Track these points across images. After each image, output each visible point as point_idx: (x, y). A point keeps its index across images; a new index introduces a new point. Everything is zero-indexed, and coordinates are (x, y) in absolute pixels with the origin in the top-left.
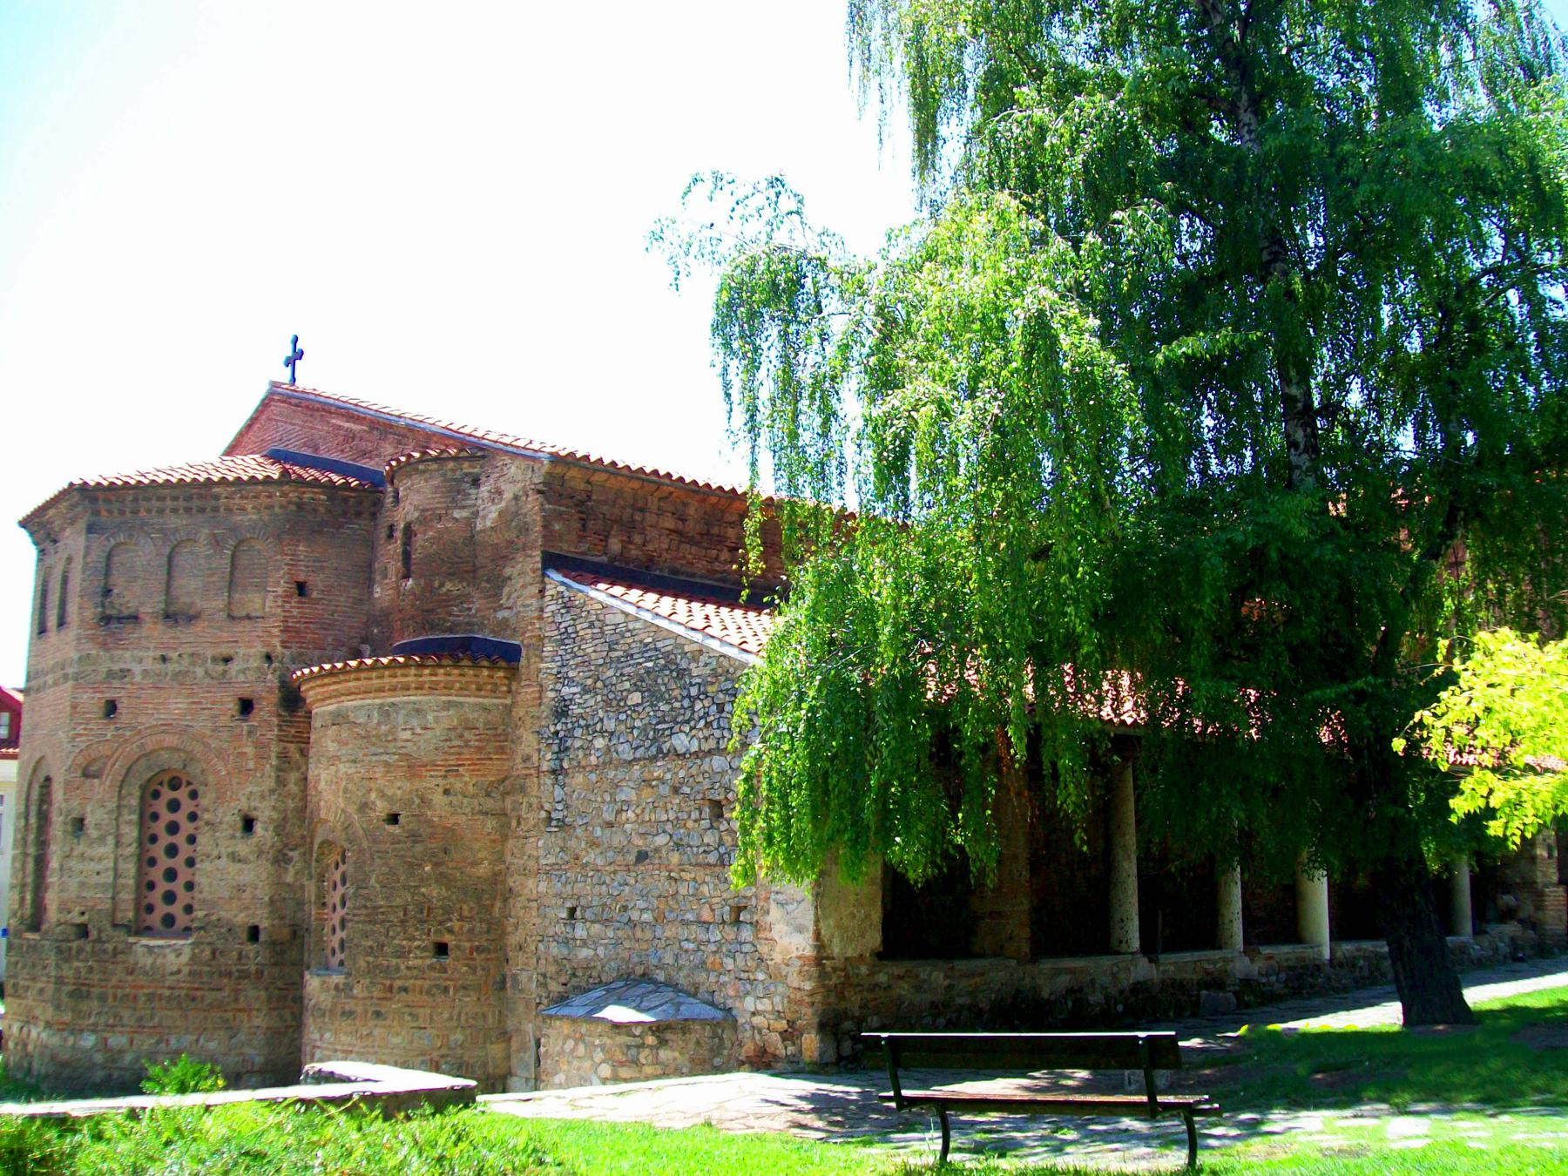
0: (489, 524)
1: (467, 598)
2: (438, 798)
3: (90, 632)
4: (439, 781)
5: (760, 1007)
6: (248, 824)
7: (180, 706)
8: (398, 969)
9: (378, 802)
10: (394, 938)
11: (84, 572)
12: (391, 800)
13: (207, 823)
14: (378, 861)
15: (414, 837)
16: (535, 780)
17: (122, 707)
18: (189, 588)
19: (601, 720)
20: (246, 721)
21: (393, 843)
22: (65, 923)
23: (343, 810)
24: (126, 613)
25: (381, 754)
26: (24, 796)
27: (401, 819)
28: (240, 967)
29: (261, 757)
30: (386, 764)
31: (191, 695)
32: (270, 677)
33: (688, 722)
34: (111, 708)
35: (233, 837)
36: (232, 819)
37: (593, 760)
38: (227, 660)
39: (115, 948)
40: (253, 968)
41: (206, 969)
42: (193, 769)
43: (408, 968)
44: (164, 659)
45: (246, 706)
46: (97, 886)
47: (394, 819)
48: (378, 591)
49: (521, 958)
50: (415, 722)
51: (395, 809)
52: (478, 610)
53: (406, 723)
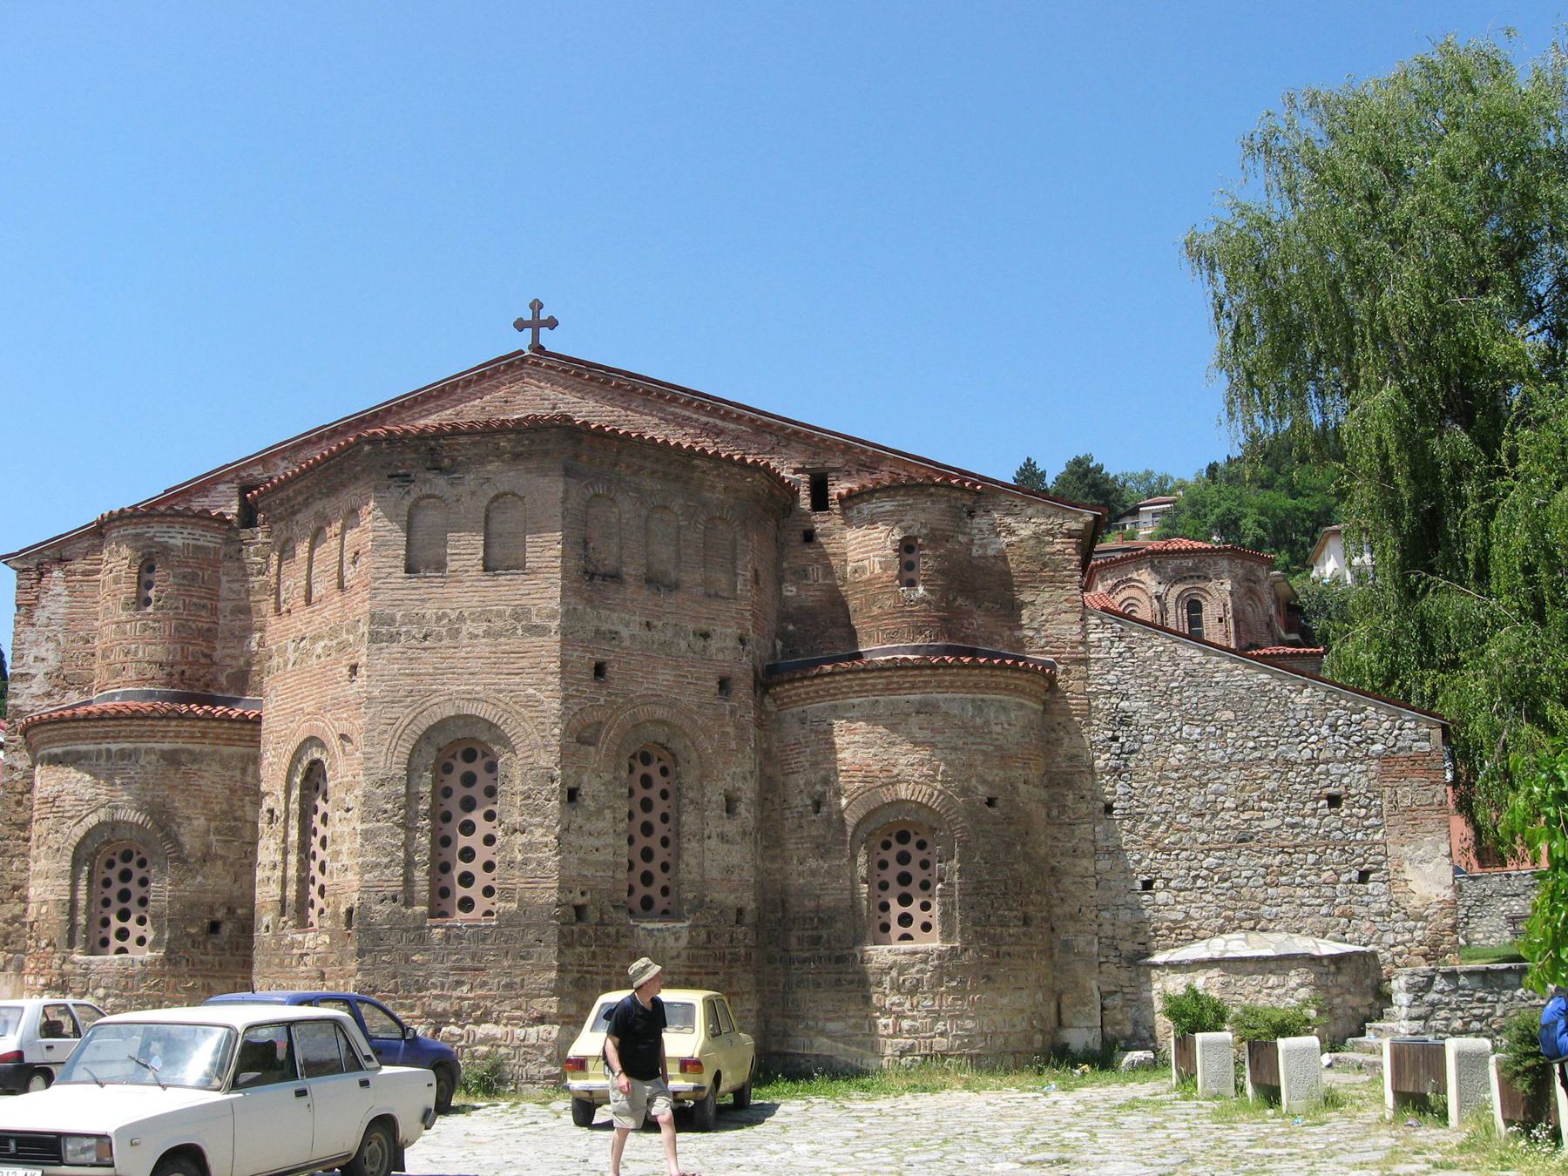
0: (990, 552)
1: (970, 614)
2: (1022, 787)
3: (576, 585)
4: (1021, 772)
5: (1399, 938)
6: (730, 805)
7: (667, 677)
8: (1002, 938)
9: (980, 787)
10: (998, 909)
11: (564, 518)
12: (991, 785)
13: (692, 802)
14: (982, 840)
15: (1009, 820)
16: (1089, 776)
17: (612, 670)
18: (664, 554)
19: (1180, 730)
20: (727, 700)
21: (994, 824)
22: (567, 904)
23: (941, 792)
24: (602, 570)
25: (980, 744)
26: (404, 758)
27: (999, 803)
28: (732, 950)
29: (742, 739)
30: (983, 752)
31: (678, 667)
32: (745, 659)
33: (1297, 736)
34: (599, 670)
35: (721, 817)
36: (715, 795)
37: (1174, 761)
38: (706, 635)
39: (617, 933)
40: (743, 951)
41: (703, 952)
42: (676, 745)
43: (1010, 935)
44: (648, 624)
45: (724, 685)
46: (596, 864)
47: (991, 802)
48: (790, 590)
49: (1072, 927)
50: (1003, 718)
51: (994, 793)
52: (980, 626)
53: (996, 718)
